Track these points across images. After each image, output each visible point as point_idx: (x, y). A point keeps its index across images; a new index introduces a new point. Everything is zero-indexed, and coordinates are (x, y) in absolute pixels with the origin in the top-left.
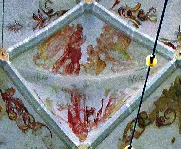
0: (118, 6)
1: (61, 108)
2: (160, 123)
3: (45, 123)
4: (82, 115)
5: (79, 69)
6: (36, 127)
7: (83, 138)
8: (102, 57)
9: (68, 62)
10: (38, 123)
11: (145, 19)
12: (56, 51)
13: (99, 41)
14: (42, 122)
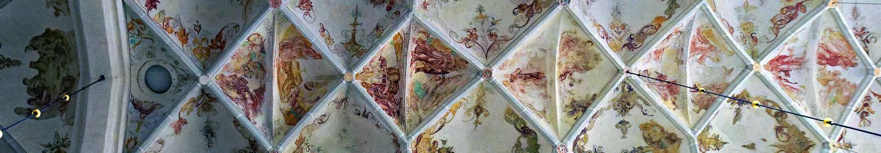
0: (872, 95)
1: (790, 50)
2: (778, 130)
3: (778, 37)
4: (785, 67)
5: (822, 64)
6: (775, 30)
7: (766, 67)
8: (832, 83)
9: (828, 56)
10: (779, 32)
11: (862, 117)
12: (836, 46)
13: (844, 80)
14: (779, 35)
